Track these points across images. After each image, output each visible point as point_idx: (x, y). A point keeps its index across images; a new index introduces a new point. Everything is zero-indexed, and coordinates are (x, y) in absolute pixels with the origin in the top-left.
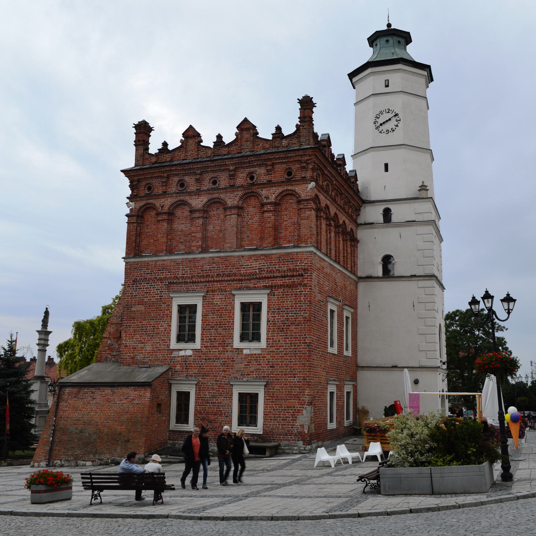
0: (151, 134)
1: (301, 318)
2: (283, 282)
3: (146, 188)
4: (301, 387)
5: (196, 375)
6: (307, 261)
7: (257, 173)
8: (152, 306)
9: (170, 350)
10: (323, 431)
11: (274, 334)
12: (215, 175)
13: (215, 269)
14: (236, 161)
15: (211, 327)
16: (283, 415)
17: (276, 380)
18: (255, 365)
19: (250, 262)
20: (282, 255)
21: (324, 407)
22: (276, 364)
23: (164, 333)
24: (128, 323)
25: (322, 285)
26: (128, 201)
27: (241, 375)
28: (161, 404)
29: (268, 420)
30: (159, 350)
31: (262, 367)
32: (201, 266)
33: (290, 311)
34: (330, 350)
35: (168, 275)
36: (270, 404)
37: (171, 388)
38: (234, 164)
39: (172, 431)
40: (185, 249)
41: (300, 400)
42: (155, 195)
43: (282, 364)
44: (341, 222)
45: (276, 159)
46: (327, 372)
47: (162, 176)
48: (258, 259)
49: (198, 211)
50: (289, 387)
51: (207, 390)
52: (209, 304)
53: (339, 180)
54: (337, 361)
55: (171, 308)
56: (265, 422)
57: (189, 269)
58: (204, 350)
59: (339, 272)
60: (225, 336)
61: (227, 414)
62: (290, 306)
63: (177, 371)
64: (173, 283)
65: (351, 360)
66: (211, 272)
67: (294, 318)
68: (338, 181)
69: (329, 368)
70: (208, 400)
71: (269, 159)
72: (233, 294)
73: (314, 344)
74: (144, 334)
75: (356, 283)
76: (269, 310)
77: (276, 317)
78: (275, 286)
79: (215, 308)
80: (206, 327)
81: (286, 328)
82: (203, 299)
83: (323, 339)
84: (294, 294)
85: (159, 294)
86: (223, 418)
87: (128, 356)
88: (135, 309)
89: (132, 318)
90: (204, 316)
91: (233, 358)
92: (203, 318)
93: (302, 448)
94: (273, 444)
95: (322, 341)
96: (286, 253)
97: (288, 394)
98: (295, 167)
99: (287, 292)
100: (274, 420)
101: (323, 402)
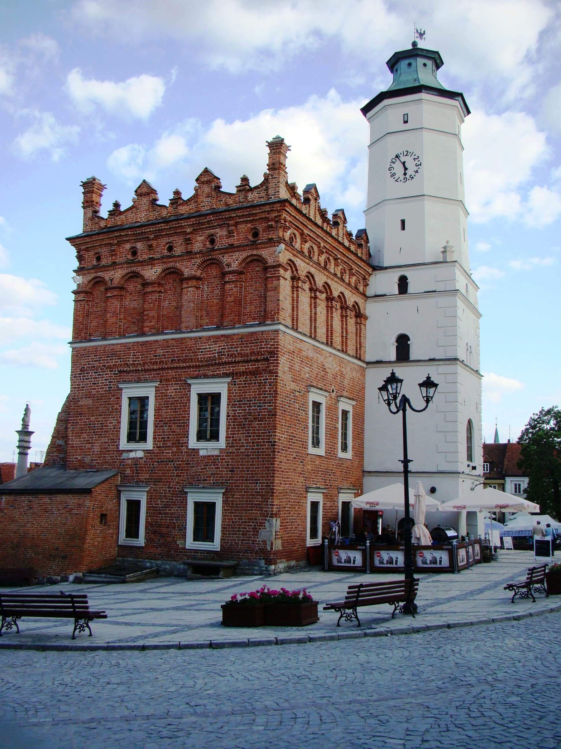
0: (102, 193)
1: (265, 412)
2: (246, 369)
3: (95, 259)
4: (264, 495)
5: (147, 482)
6: (274, 342)
7: (218, 235)
8: (100, 399)
9: (119, 451)
10: (298, 548)
11: (234, 431)
12: (171, 239)
13: (170, 353)
14: (193, 221)
15: (164, 424)
16: (243, 528)
17: (235, 486)
18: (213, 468)
19: (209, 345)
20: (246, 335)
21: (301, 519)
22: (236, 468)
23: (113, 431)
24: (74, 420)
25: (299, 371)
26: (75, 274)
27: (197, 481)
28: (106, 515)
29: (226, 534)
30: (108, 451)
31: (220, 471)
32: (154, 351)
33: (253, 404)
34: (312, 450)
35: (118, 362)
36: (228, 516)
37: (120, 495)
38: (190, 225)
39: (121, 546)
40: (137, 331)
41: (262, 511)
42: (104, 266)
43: (243, 468)
44: (336, 294)
45: (239, 217)
46: (306, 477)
47: (111, 243)
48: (218, 341)
49: (152, 284)
50: (250, 495)
51: (159, 499)
52: (162, 396)
53: (328, 241)
54: (326, 464)
55: (121, 401)
56: (223, 536)
57: (141, 355)
58: (157, 450)
59: (330, 356)
60: (179, 434)
61: (180, 527)
62: (253, 398)
63: (127, 476)
64: (124, 371)
65: (352, 463)
66: (165, 358)
67: (258, 412)
68: (329, 243)
69: (310, 472)
70: (160, 510)
71: (231, 218)
72: (189, 384)
73: (282, 443)
74: (91, 432)
75: (364, 369)
76: (229, 402)
77: (236, 410)
78: (237, 373)
79: (169, 401)
80: (158, 424)
81: (247, 424)
82: (156, 391)
83: (299, 438)
84: (258, 383)
85: (107, 385)
86: (175, 532)
87: (75, 458)
88: (82, 403)
89: (80, 414)
90: (157, 410)
91: (188, 461)
92: (155, 413)
93: (264, 569)
94: (231, 563)
95: (297, 440)
96: (250, 333)
97: (249, 504)
98: (260, 227)
99: (250, 380)
100: (232, 534)
101: (299, 514)
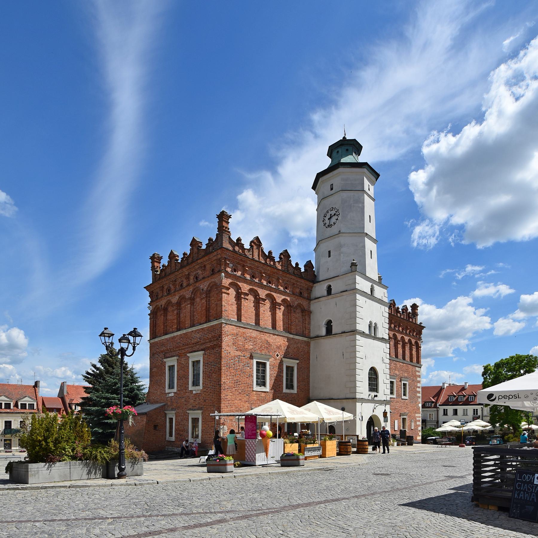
81: (211, 376)
